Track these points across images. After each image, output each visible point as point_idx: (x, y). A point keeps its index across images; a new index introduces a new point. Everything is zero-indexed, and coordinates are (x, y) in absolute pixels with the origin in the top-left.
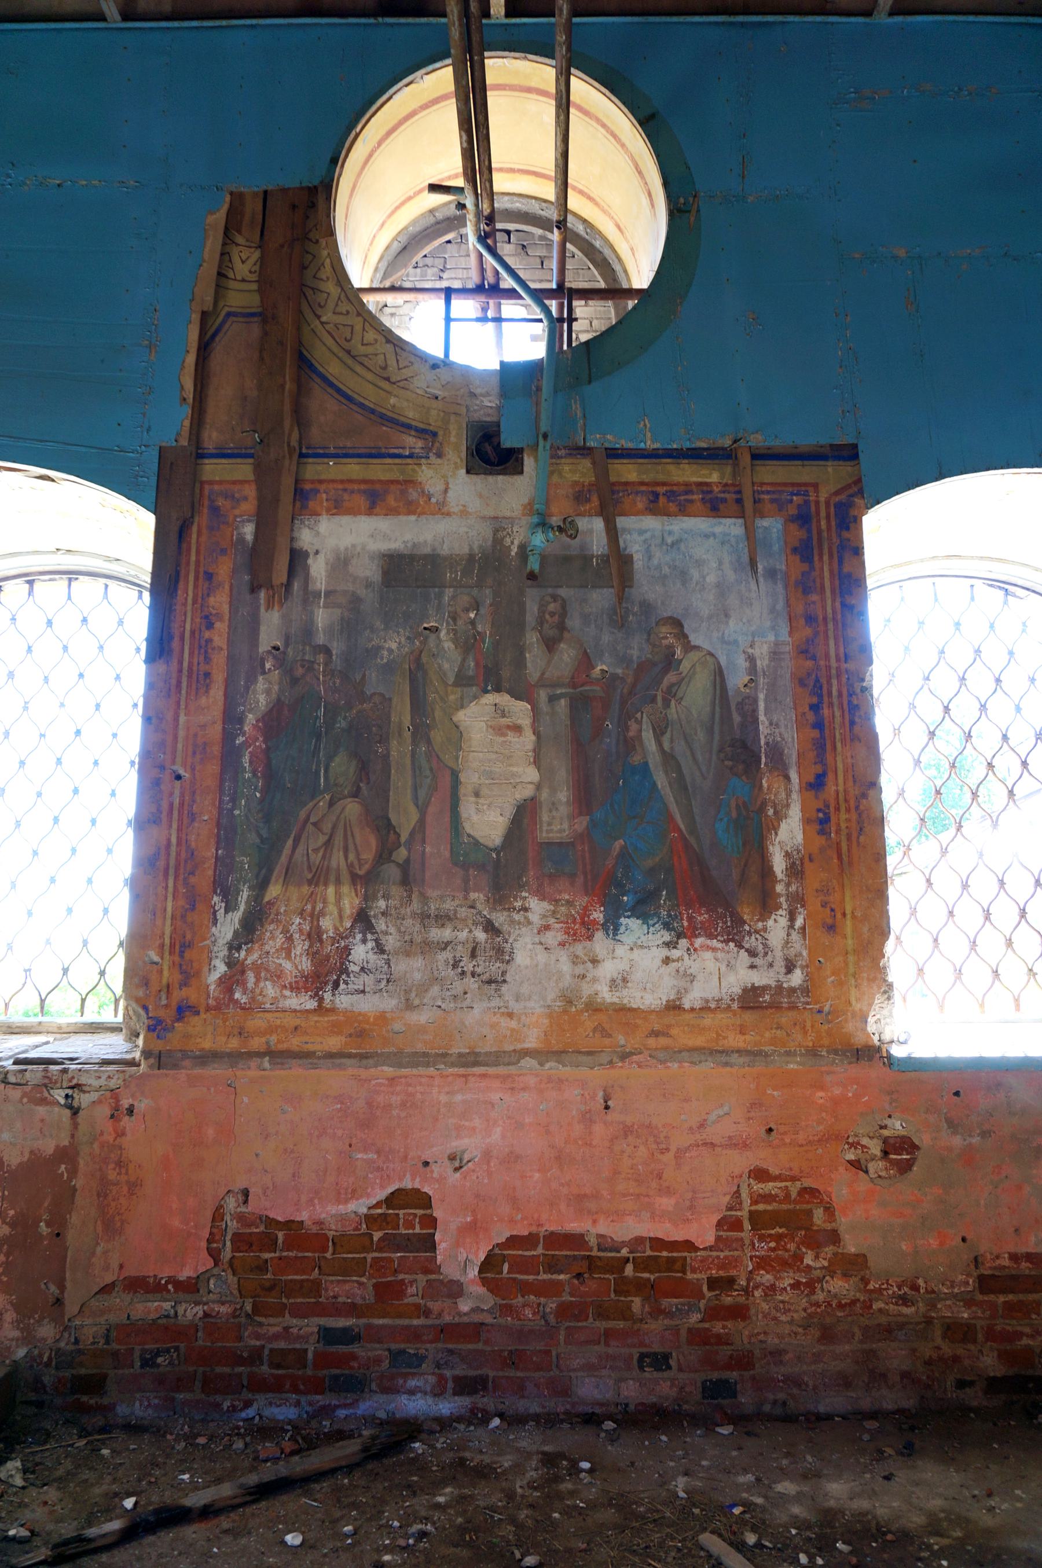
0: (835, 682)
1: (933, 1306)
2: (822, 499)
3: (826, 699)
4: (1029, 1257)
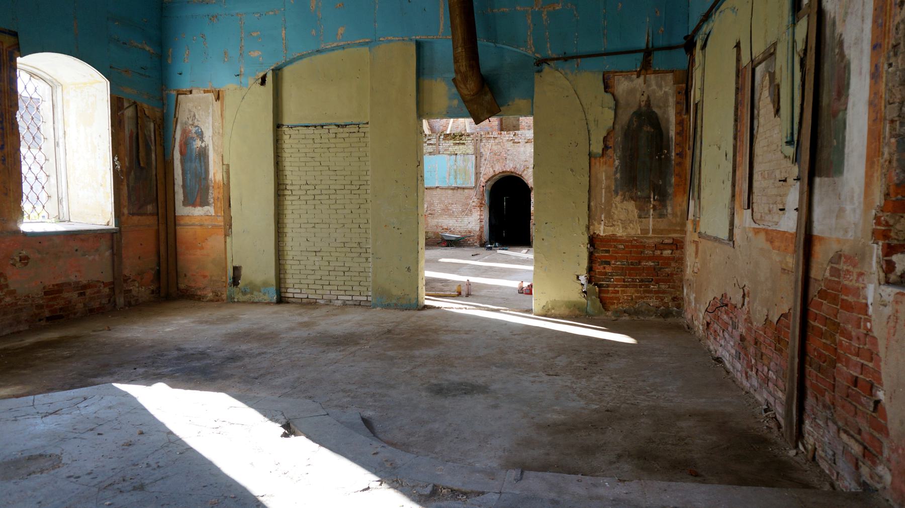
0: (7, 114)
1: (33, 301)
2: (4, 48)
3: (4, 119)
4: (57, 285)
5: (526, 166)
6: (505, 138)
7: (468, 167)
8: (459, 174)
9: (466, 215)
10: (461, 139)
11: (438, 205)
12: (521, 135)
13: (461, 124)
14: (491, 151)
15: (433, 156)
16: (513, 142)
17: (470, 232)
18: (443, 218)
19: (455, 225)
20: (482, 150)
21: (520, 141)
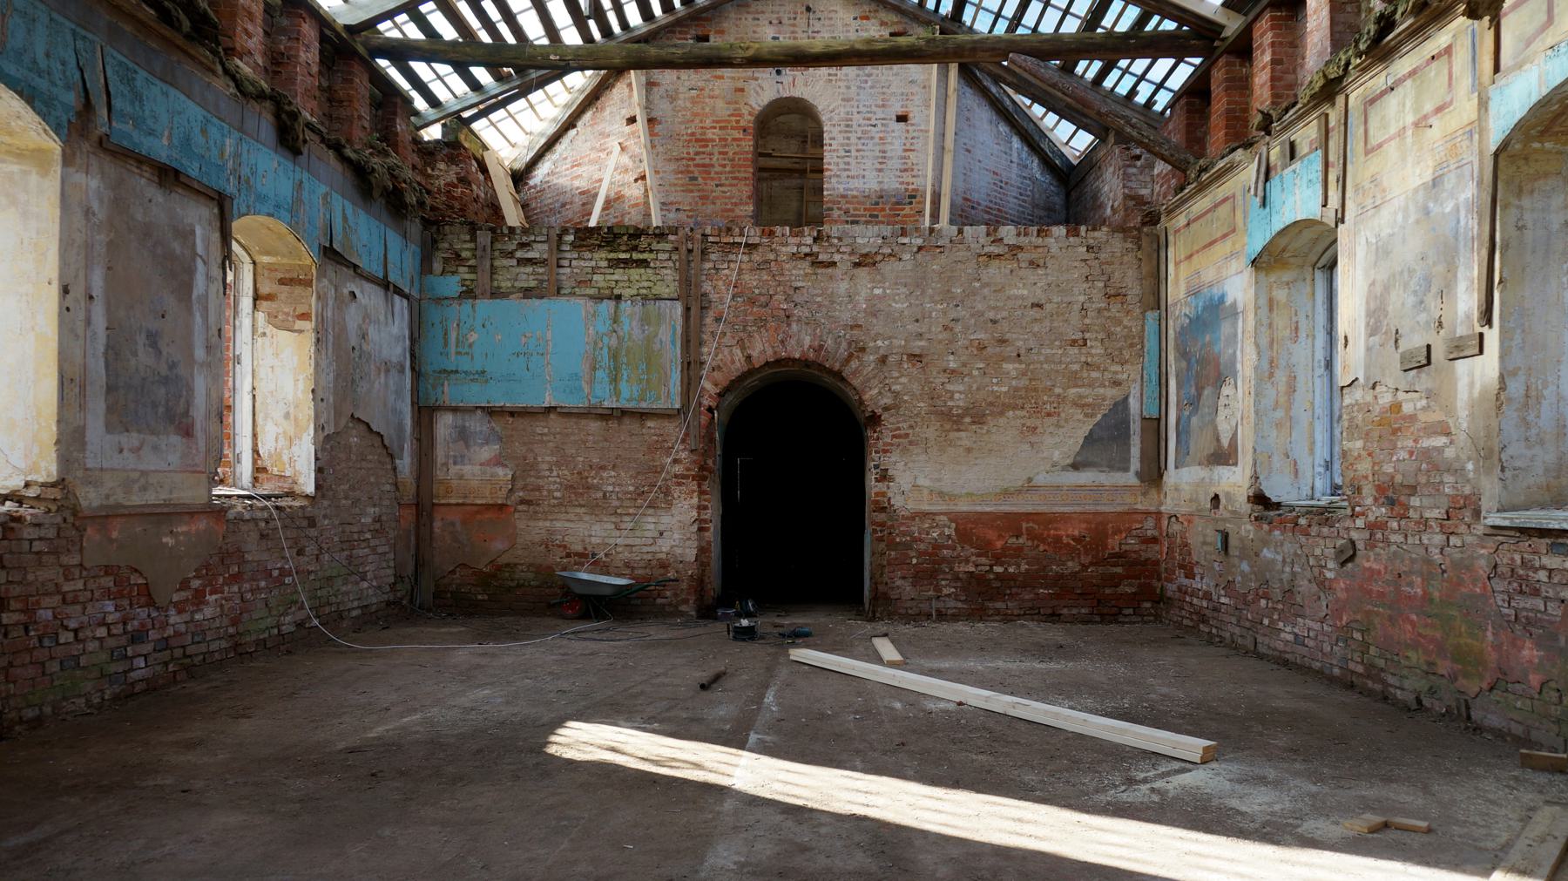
5: (856, 342)
6: (784, 249)
7: (657, 340)
8: (627, 364)
9: (649, 507)
10: (635, 248)
11: (551, 470)
12: (840, 239)
13: (633, 211)
14: (739, 290)
15: (536, 302)
16: (813, 263)
17: (664, 565)
18: (571, 516)
19: (611, 541)
20: (707, 287)
21: (837, 257)
